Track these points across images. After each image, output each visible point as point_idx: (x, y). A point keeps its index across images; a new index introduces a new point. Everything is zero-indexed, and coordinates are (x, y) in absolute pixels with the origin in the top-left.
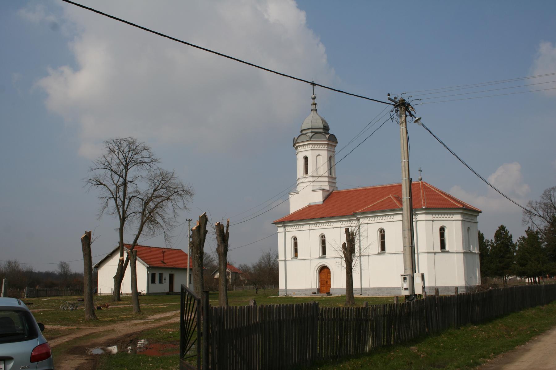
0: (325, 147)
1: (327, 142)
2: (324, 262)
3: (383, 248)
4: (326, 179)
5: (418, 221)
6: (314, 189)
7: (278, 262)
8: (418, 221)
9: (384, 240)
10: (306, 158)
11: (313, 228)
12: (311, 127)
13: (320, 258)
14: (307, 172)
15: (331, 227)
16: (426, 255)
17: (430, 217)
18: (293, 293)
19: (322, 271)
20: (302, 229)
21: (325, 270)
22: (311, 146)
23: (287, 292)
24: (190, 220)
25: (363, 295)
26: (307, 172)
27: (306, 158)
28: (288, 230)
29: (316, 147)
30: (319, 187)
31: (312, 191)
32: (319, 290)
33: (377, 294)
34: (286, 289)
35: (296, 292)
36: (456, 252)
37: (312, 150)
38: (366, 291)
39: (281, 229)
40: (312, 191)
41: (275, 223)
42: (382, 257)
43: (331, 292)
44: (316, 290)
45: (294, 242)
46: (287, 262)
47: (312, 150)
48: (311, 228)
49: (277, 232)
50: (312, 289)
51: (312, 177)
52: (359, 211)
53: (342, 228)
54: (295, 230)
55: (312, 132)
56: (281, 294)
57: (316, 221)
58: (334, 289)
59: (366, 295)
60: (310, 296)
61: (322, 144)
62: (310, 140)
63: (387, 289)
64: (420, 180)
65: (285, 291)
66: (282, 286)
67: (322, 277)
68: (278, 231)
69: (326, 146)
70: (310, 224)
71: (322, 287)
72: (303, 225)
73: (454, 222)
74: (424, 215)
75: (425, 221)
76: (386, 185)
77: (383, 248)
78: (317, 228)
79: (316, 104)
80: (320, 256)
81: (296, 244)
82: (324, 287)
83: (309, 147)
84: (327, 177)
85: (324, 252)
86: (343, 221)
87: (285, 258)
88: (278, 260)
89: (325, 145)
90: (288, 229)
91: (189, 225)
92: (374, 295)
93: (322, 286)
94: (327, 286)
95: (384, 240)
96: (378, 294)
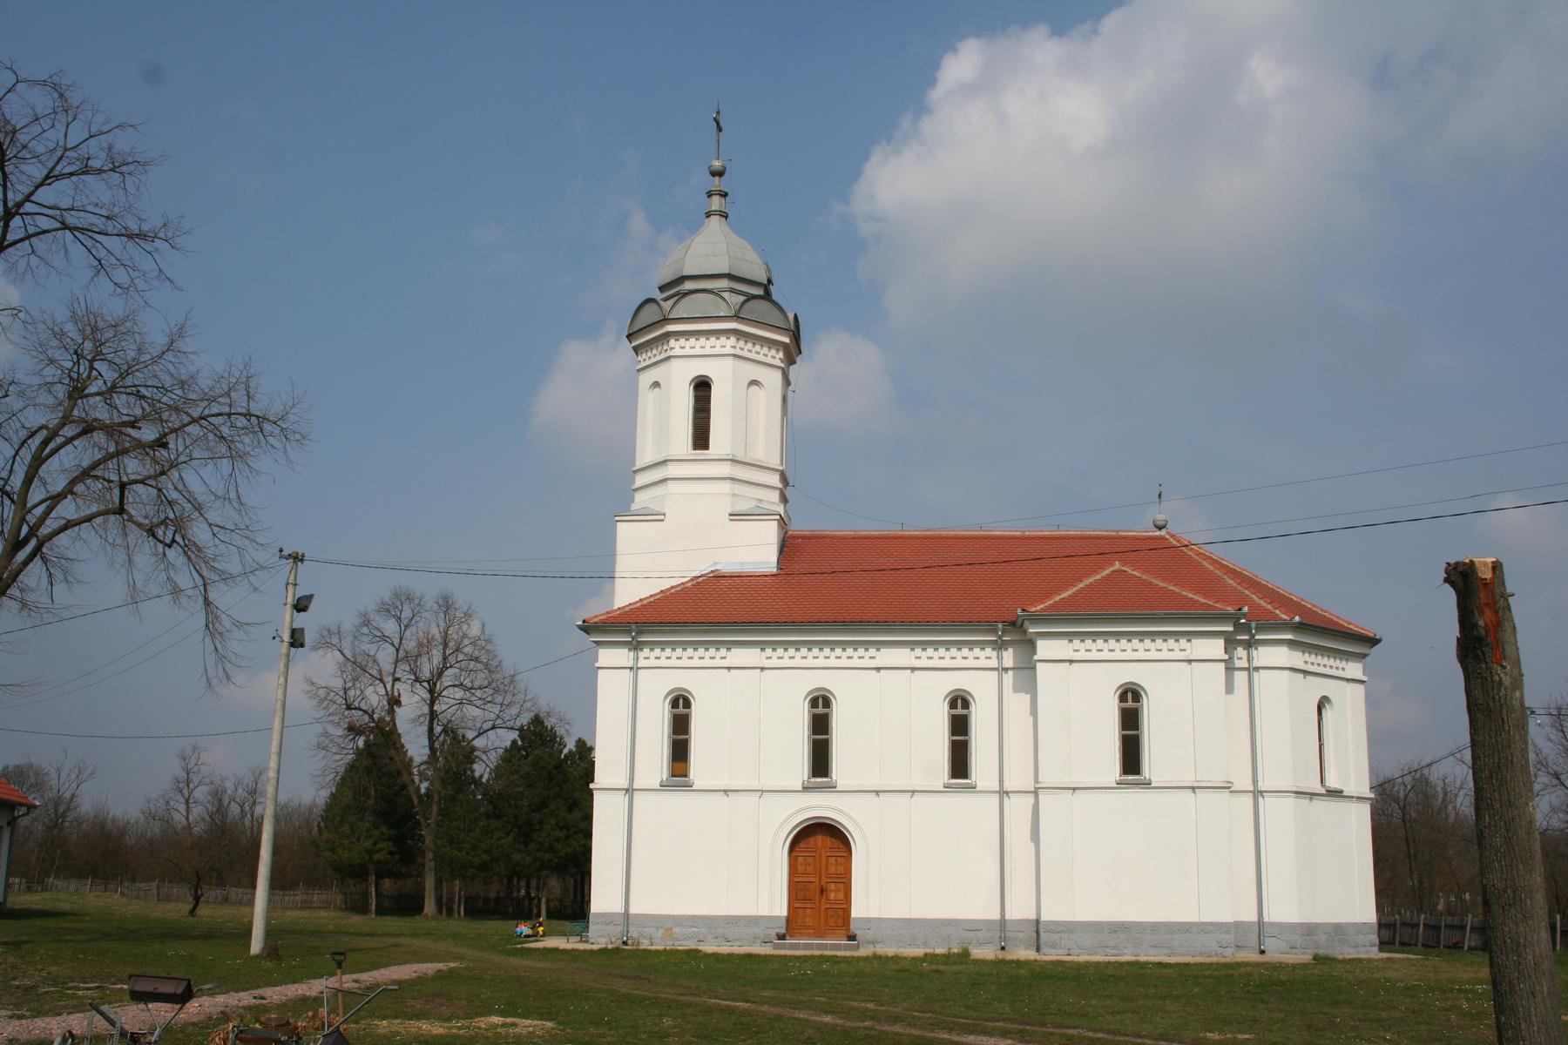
0: (777, 357)
1: (787, 340)
2: (821, 806)
3: (1131, 759)
4: (775, 480)
5: (1257, 669)
6: (743, 507)
7: (592, 795)
8: (1257, 669)
9: (824, 737)
10: (702, 387)
11: (775, 662)
12: (727, 272)
13: (664, 786)
14: (701, 438)
15: (867, 663)
16: (1291, 801)
17: (1297, 659)
18: (661, 932)
19: (802, 845)
20: (724, 663)
21: (820, 840)
22: (733, 340)
23: (631, 930)
24: (297, 558)
25: (1043, 950)
26: (701, 438)
27: (702, 387)
28: (652, 662)
29: (748, 349)
30: (754, 504)
31: (731, 515)
32: (793, 925)
33: (1107, 950)
34: (627, 915)
35: (677, 930)
36: (1358, 798)
37: (735, 356)
38: (1056, 936)
39: (621, 656)
40: (731, 515)
41: (587, 628)
42: (1133, 798)
43: (854, 928)
44: (784, 924)
45: (671, 717)
46: (637, 796)
47: (735, 356)
48: (768, 663)
49: (597, 665)
50: (762, 917)
51: (732, 460)
52: (1039, 608)
53: (916, 672)
54: (685, 662)
55: (732, 291)
56: (599, 937)
57: (800, 632)
58: (870, 920)
59: (1061, 951)
60: (766, 950)
61: (771, 343)
62: (736, 317)
63: (1155, 927)
64: (1160, 528)
65: (620, 920)
66: (604, 897)
67: (800, 869)
68: (597, 661)
69: (781, 355)
70: (763, 645)
71: (800, 911)
72: (730, 645)
73: (1352, 685)
74: (1284, 650)
75: (1287, 672)
76: (1023, 532)
77: (1131, 759)
78: (797, 662)
79: (725, 195)
80: (662, 781)
81: (680, 725)
82: (808, 911)
83: (728, 345)
84: (776, 470)
85: (820, 762)
86: (924, 645)
87: (632, 779)
88: (592, 786)
89: (778, 350)
90: (648, 657)
91: (291, 580)
92: (1096, 953)
93: (797, 905)
94: (824, 906)
95: (824, 737)
96: (1114, 948)
